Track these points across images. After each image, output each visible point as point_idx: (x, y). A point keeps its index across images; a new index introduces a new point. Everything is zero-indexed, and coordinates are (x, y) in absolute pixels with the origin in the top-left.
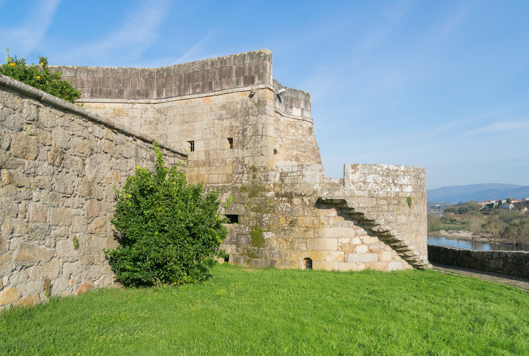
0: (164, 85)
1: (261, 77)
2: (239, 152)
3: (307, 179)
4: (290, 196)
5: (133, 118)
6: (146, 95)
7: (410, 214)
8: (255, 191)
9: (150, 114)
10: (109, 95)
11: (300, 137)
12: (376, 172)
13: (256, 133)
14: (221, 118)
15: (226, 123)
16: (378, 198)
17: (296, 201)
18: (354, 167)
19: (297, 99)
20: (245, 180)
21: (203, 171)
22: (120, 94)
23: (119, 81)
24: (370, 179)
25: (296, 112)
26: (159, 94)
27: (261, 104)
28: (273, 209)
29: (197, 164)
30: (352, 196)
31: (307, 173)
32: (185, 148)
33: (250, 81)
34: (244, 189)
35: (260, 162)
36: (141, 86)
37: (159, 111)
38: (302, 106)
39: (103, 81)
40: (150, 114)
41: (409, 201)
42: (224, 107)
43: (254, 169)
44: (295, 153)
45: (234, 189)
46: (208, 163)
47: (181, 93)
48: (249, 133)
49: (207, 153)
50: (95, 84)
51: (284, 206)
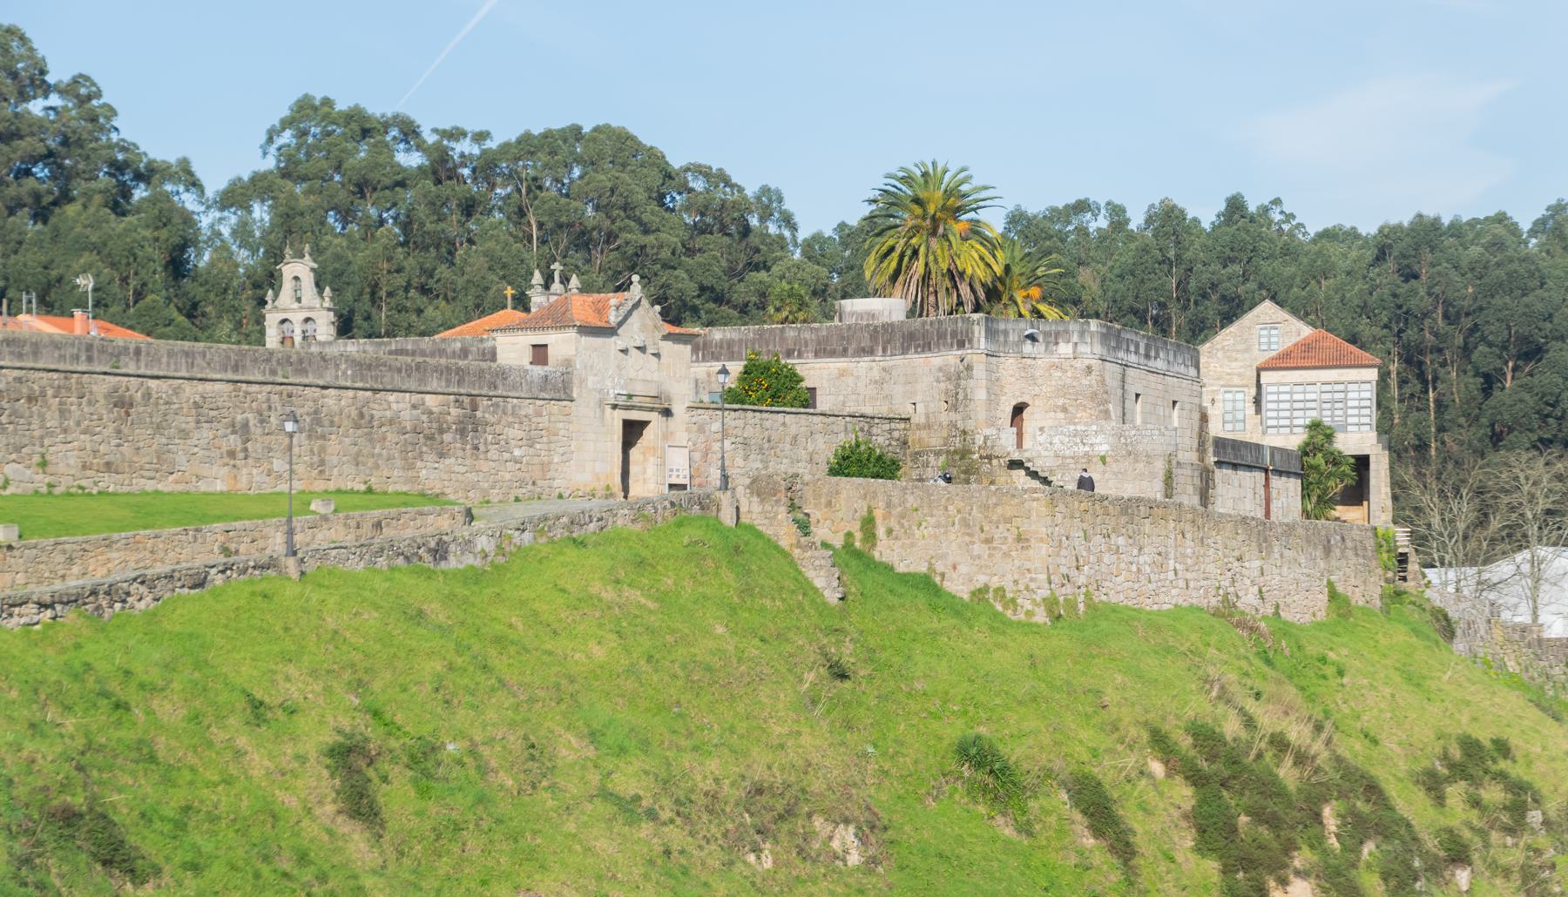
0: (889, 342)
1: (970, 341)
2: (953, 416)
3: (1003, 442)
4: (989, 458)
5: (858, 377)
6: (871, 352)
7: (1104, 473)
8: (964, 453)
9: (876, 374)
10: (832, 354)
11: (1069, 381)
12: (1062, 433)
13: (966, 397)
14: (938, 381)
15: (942, 386)
16: (1064, 457)
17: (995, 462)
18: (1041, 429)
19: (1067, 332)
20: (957, 443)
21: (924, 434)
22: (844, 353)
23: (843, 338)
24: (1056, 440)
25: (1065, 349)
26: (884, 350)
27: (969, 368)
28: (977, 471)
29: (919, 427)
30: (1039, 456)
31: (1003, 436)
32: (907, 410)
33: (961, 345)
34: (956, 452)
35: (970, 425)
36: (866, 343)
37: (884, 369)
38: (1075, 338)
39: (827, 339)
40: (876, 374)
41: (1103, 459)
42: (940, 369)
43: (964, 432)
44: (1060, 402)
45: (948, 452)
46: (928, 426)
47: (905, 351)
48: (961, 397)
49: (927, 417)
50: (819, 343)
51: (985, 468)
